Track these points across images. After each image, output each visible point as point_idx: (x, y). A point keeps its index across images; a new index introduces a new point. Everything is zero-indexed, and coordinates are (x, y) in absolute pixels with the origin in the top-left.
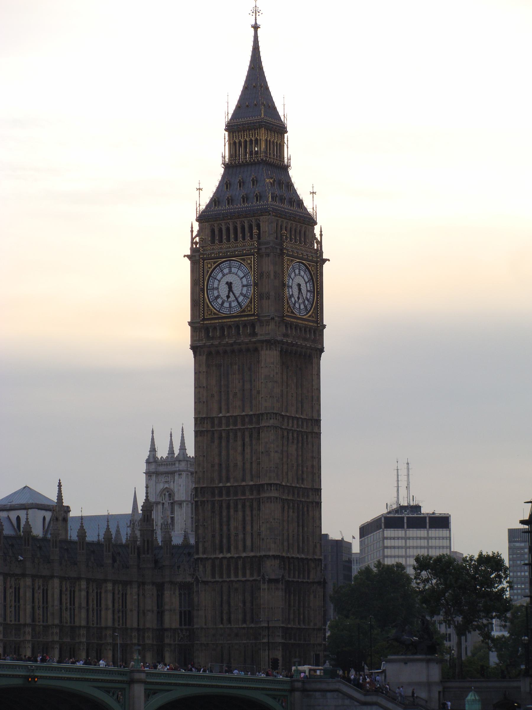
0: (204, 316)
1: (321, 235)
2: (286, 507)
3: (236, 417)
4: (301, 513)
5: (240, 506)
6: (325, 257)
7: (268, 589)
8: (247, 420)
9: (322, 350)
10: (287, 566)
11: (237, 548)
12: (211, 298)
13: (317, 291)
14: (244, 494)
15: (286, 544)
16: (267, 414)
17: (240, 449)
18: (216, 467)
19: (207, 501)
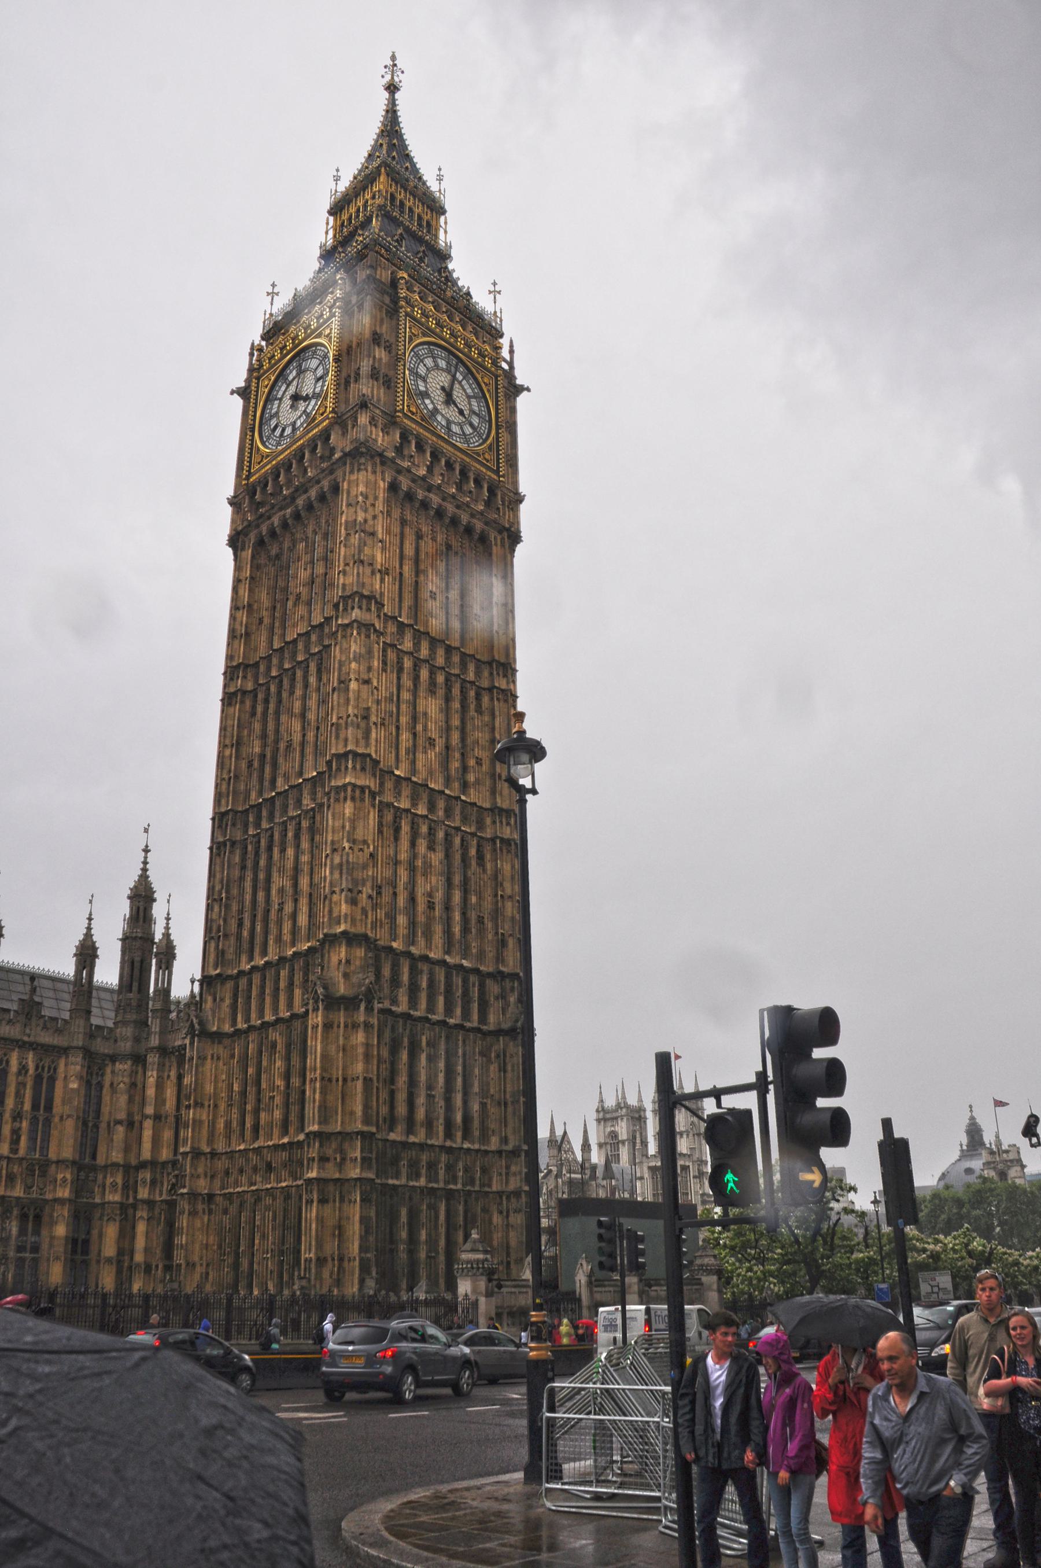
0: (249, 471)
1: (511, 352)
2: (405, 828)
3: (295, 641)
4: (457, 857)
5: (290, 834)
6: (518, 382)
7: (328, 1026)
8: (314, 638)
9: (514, 538)
10: (405, 978)
11: (279, 939)
12: (266, 432)
13: (497, 421)
14: (299, 802)
15: (402, 920)
16: (345, 598)
17: (297, 705)
18: (256, 764)
19: (233, 844)
